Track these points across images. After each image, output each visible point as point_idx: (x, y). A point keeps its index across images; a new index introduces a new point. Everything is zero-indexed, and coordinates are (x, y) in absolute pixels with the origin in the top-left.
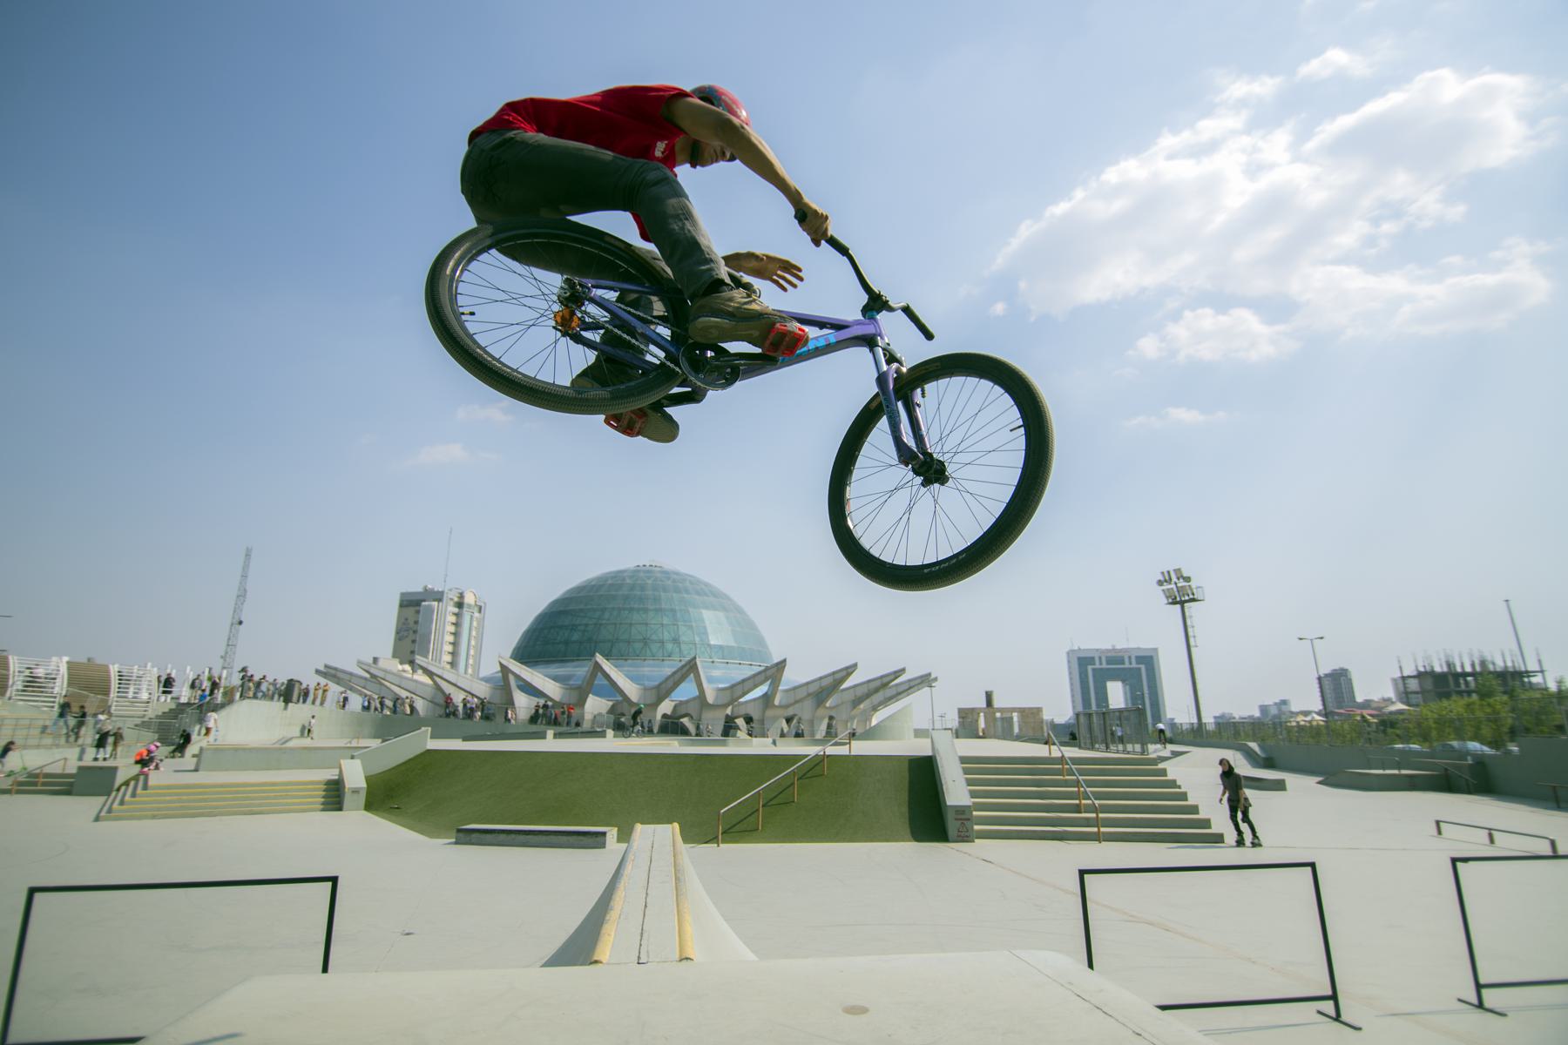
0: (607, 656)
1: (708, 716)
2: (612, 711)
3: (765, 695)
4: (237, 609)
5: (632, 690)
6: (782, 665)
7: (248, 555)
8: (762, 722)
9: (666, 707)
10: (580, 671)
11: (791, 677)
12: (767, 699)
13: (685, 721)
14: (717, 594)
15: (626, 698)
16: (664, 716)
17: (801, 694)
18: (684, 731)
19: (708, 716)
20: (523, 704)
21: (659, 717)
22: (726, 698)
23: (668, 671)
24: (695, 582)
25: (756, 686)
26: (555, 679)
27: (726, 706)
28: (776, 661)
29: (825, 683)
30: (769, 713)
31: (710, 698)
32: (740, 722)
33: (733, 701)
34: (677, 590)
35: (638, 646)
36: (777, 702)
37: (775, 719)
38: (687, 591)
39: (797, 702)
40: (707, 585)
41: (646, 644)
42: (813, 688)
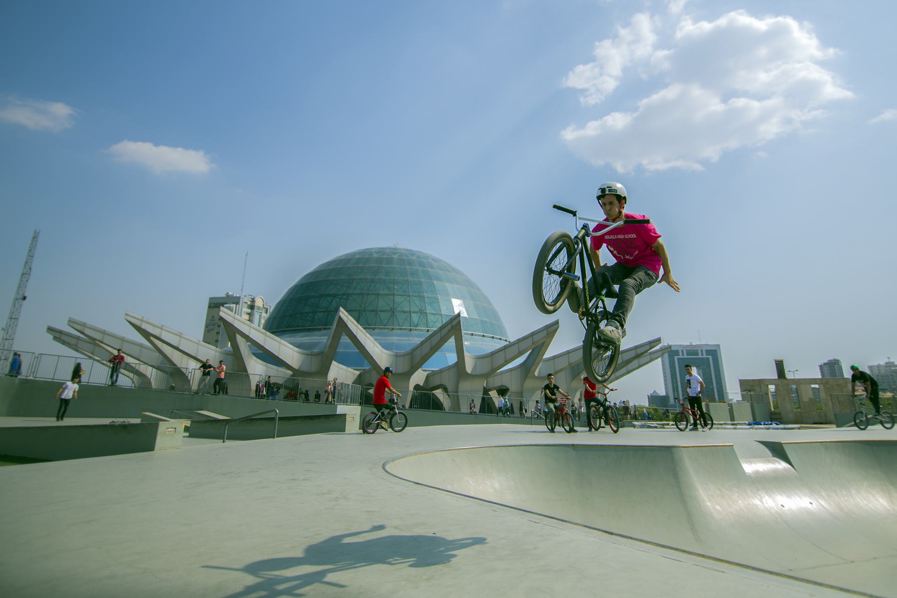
2: (359, 380)
4: (22, 286)
5: (382, 357)
7: (35, 238)
8: (521, 394)
9: (418, 378)
10: (321, 339)
12: (526, 369)
13: (439, 393)
16: (417, 387)
17: (563, 363)
19: (465, 386)
20: (257, 369)
21: (411, 388)
22: (485, 368)
23: (417, 341)
26: (299, 346)
30: (529, 384)
31: (469, 369)
35: (383, 315)
36: (536, 374)
37: (533, 391)
41: (393, 313)
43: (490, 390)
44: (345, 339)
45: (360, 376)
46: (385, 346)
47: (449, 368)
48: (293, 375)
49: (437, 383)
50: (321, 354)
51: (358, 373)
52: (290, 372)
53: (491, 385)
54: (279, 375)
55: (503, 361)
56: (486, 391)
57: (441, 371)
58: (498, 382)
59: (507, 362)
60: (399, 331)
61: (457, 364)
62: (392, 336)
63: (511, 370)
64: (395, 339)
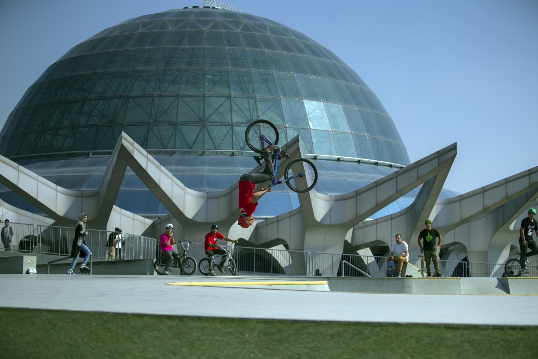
0: (161, 151)
1: (313, 240)
2: (150, 232)
3: (411, 209)
6: (445, 158)
11: (459, 181)
14: (316, 50)
15: (176, 213)
18: (270, 268)
22: (349, 214)
24: (280, 31)
25: (399, 193)
27: (345, 227)
28: (417, 148)
29: (514, 189)
32: (366, 255)
33: (356, 221)
34: (253, 42)
38: (269, 45)
39: (464, 221)
40: (299, 36)
42: (492, 199)
43: (360, 247)
44: (130, 172)
45: (153, 226)
46: (190, 182)
47: (291, 215)
48: (54, 224)
49: (272, 237)
50: (96, 195)
51: (149, 222)
52: (50, 221)
53: (360, 240)
54: (39, 224)
55: (372, 205)
56: (350, 249)
57: (278, 220)
58: (371, 236)
59: (379, 206)
60: (213, 157)
61: (300, 211)
62: (202, 164)
63: (392, 217)
64: (206, 170)
